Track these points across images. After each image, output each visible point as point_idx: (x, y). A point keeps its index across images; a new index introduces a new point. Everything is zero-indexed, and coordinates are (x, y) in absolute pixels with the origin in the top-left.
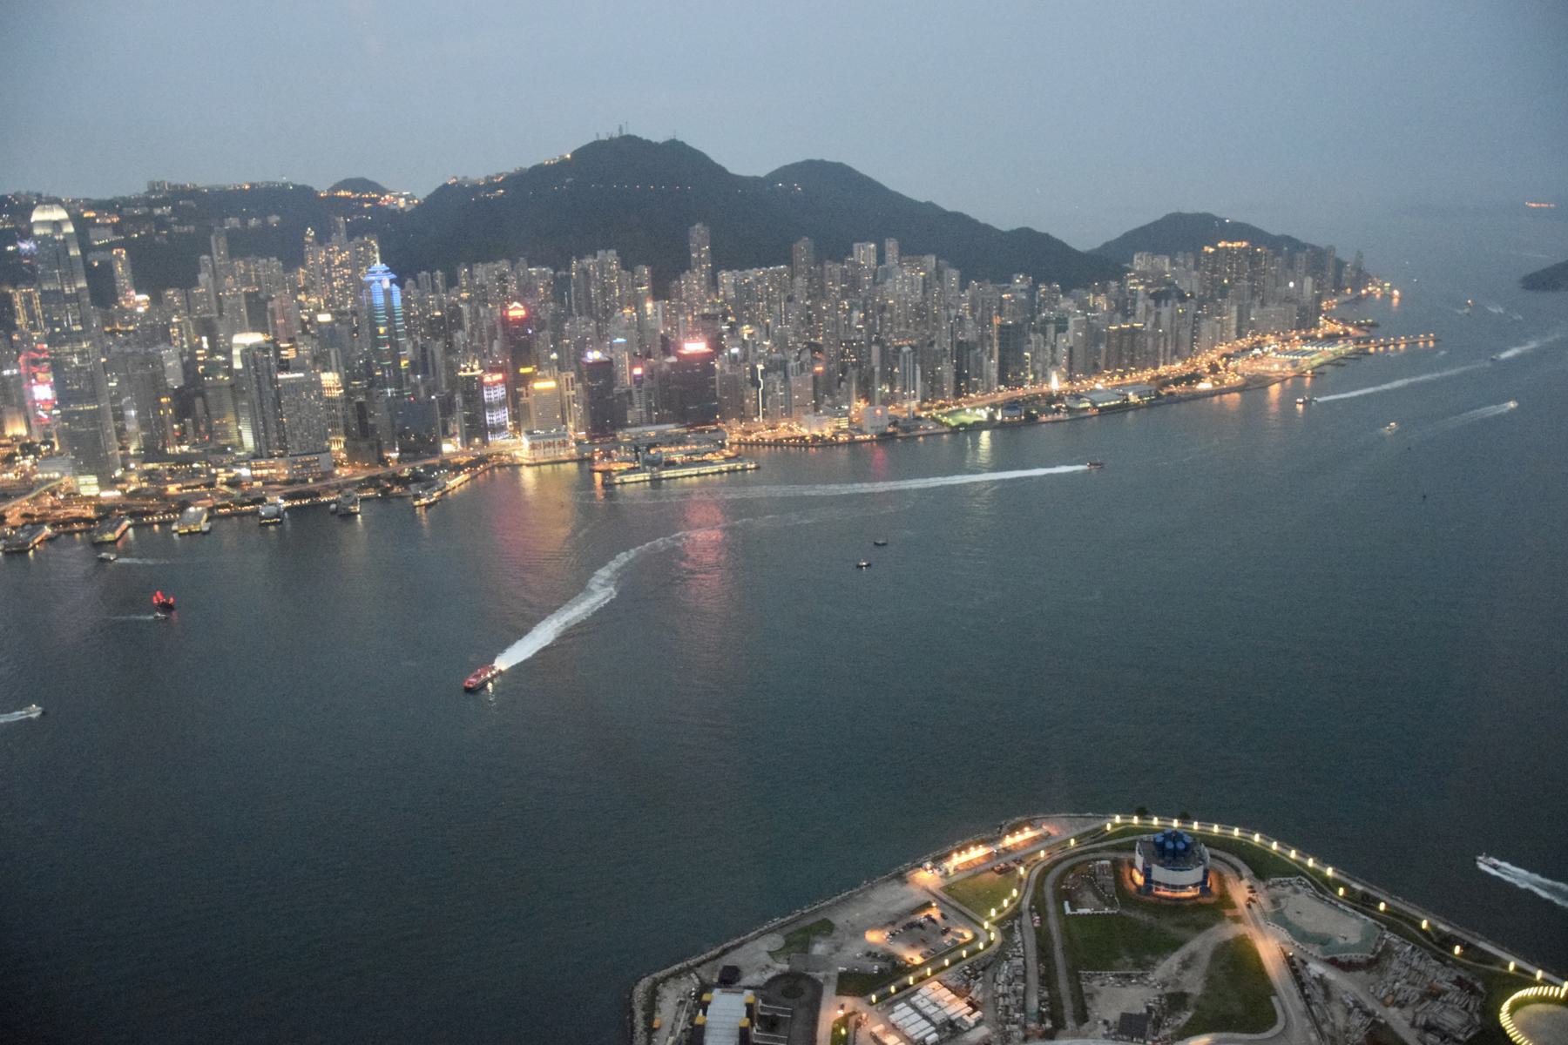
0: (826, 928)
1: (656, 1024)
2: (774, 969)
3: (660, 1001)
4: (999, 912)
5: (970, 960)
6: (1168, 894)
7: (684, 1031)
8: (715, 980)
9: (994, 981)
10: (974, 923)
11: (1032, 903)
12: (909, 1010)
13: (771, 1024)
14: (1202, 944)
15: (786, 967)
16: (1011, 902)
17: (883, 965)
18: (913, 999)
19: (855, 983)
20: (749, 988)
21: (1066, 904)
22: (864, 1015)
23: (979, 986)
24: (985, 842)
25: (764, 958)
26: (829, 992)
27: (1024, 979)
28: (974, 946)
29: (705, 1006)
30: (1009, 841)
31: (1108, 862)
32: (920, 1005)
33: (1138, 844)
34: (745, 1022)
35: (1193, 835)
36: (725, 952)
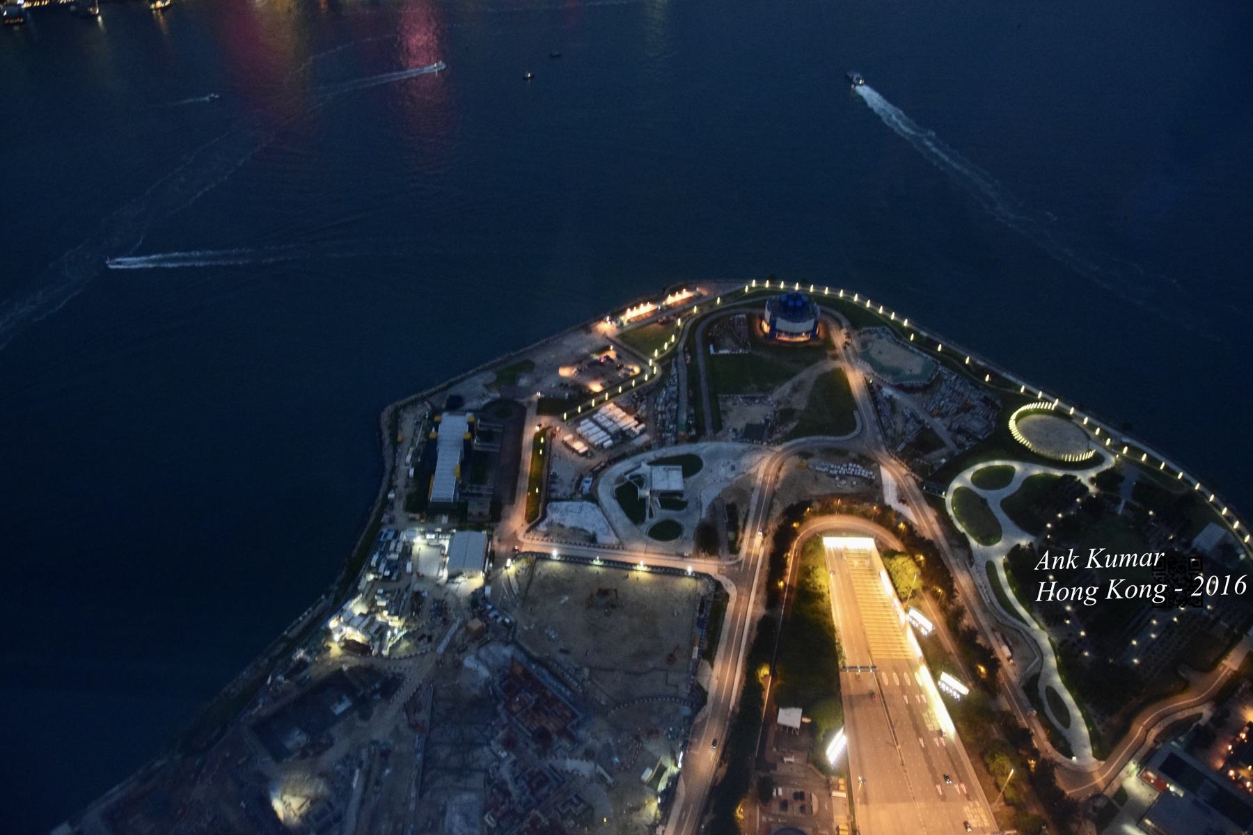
0: (529, 367)
1: (400, 438)
2: (489, 397)
3: (401, 422)
4: (661, 352)
5: (638, 387)
6: (786, 339)
7: (420, 444)
8: (444, 406)
9: (655, 401)
10: (642, 361)
11: (685, 347)
12: (591, 424)
13: (487, 436)
14: (808, 375)
15: (498, 395)
16: (669, 346)
17: (572, 392)
18: (595, 417)
19: (550, 406)
20: (470, 411)
21: (711, 348)
22: (558, 429)
23: (644, 407)
24: (653, 302)
25: (480, 388)
26: (531, 412)
27: (677, 401)
28: (641, 378)
29: (437, 425)
30: (670, 300)
31: (744, 316)
32: (600, 420)
33: (767, 303)
34: (468, 436)
35: (810, 296)
36: (450, 385)
